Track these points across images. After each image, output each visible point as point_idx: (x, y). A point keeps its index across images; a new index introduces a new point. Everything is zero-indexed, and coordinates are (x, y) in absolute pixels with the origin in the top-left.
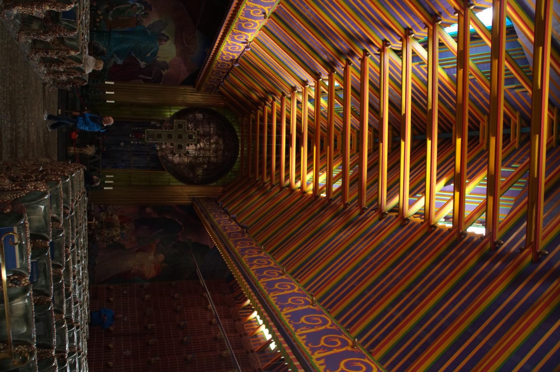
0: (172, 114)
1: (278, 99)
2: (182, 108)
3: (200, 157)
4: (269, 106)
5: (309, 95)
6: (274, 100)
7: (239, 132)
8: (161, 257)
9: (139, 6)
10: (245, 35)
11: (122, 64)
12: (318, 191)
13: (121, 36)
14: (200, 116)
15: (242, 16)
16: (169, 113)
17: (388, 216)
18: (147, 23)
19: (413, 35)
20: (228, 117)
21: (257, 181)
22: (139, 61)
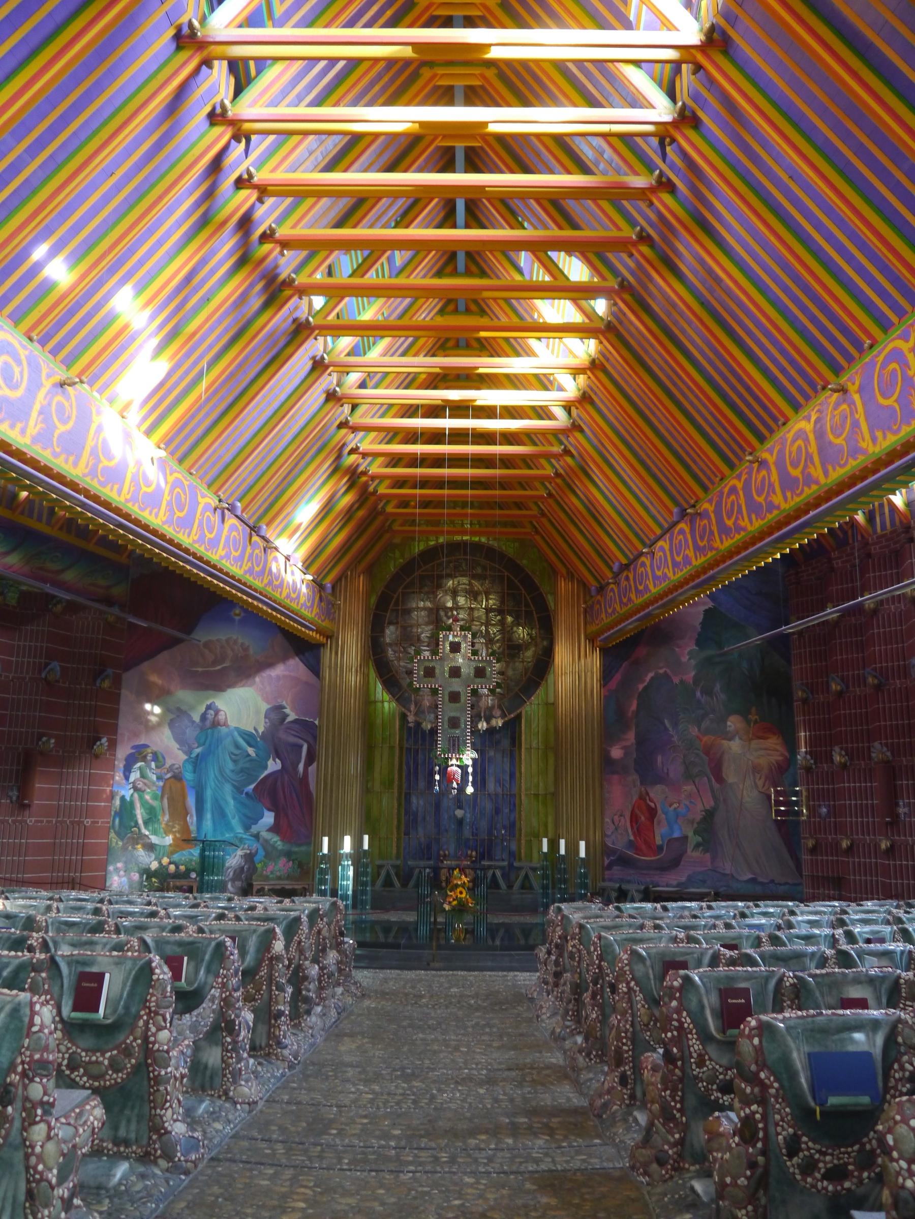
0: (386, 697)
1: (353, 440)
2: (373, 674)
3: (487, 630)
4: (369, 465)
5: (348, 355)
6: (353, 451)
7: (428, 540)
8: (734, 723)
9: (138, 774)
10: (203, 514)
11: (272, 814)
12: (593, 325)
13: (208, 816)
14: (390, 633)
15: (157, 516)
16: (386, 704)
17: (690, 102)
18: (177, 756)
19: (196, 23)
20: (392, 568)
21: (550, 495)
22: (266, 773)
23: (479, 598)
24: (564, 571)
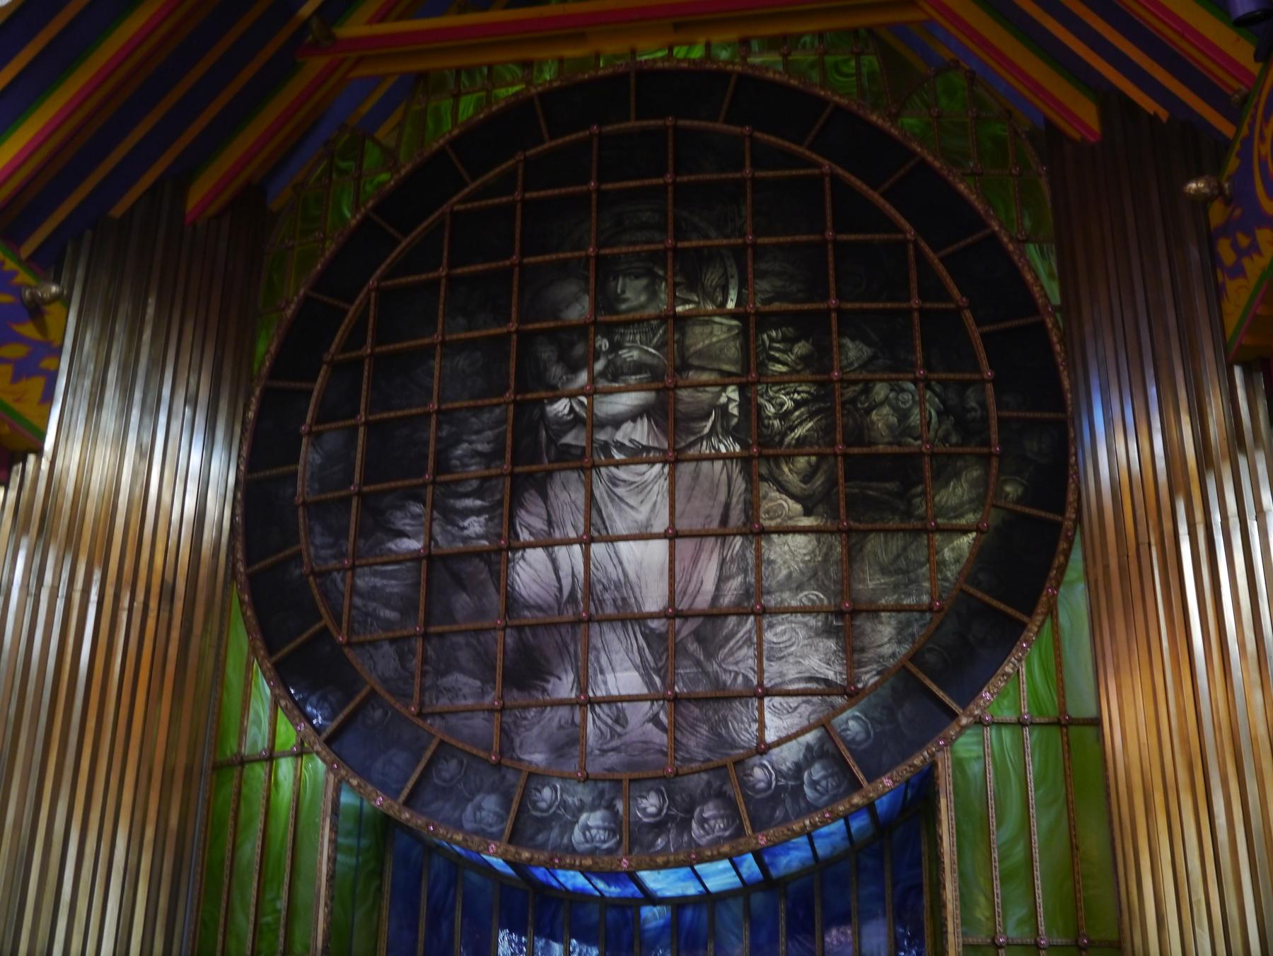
0: (287, 734)
2: (239, 640)
3: (745, 404)
23: (712, 278)
24: (1088, 113)
